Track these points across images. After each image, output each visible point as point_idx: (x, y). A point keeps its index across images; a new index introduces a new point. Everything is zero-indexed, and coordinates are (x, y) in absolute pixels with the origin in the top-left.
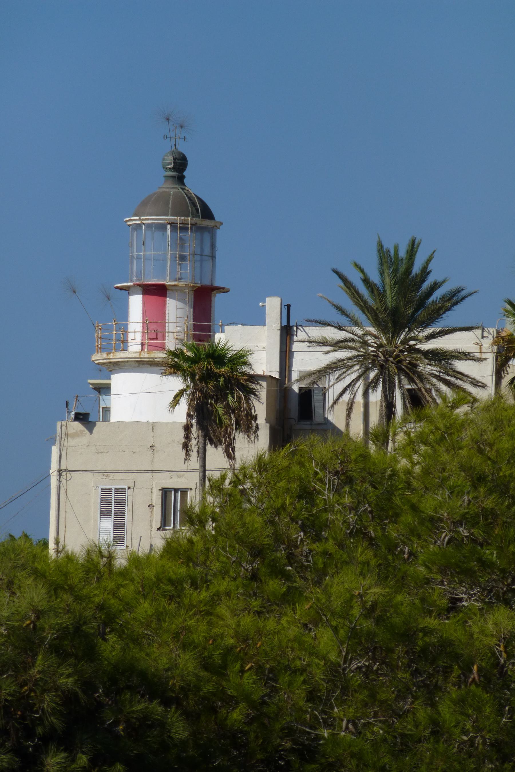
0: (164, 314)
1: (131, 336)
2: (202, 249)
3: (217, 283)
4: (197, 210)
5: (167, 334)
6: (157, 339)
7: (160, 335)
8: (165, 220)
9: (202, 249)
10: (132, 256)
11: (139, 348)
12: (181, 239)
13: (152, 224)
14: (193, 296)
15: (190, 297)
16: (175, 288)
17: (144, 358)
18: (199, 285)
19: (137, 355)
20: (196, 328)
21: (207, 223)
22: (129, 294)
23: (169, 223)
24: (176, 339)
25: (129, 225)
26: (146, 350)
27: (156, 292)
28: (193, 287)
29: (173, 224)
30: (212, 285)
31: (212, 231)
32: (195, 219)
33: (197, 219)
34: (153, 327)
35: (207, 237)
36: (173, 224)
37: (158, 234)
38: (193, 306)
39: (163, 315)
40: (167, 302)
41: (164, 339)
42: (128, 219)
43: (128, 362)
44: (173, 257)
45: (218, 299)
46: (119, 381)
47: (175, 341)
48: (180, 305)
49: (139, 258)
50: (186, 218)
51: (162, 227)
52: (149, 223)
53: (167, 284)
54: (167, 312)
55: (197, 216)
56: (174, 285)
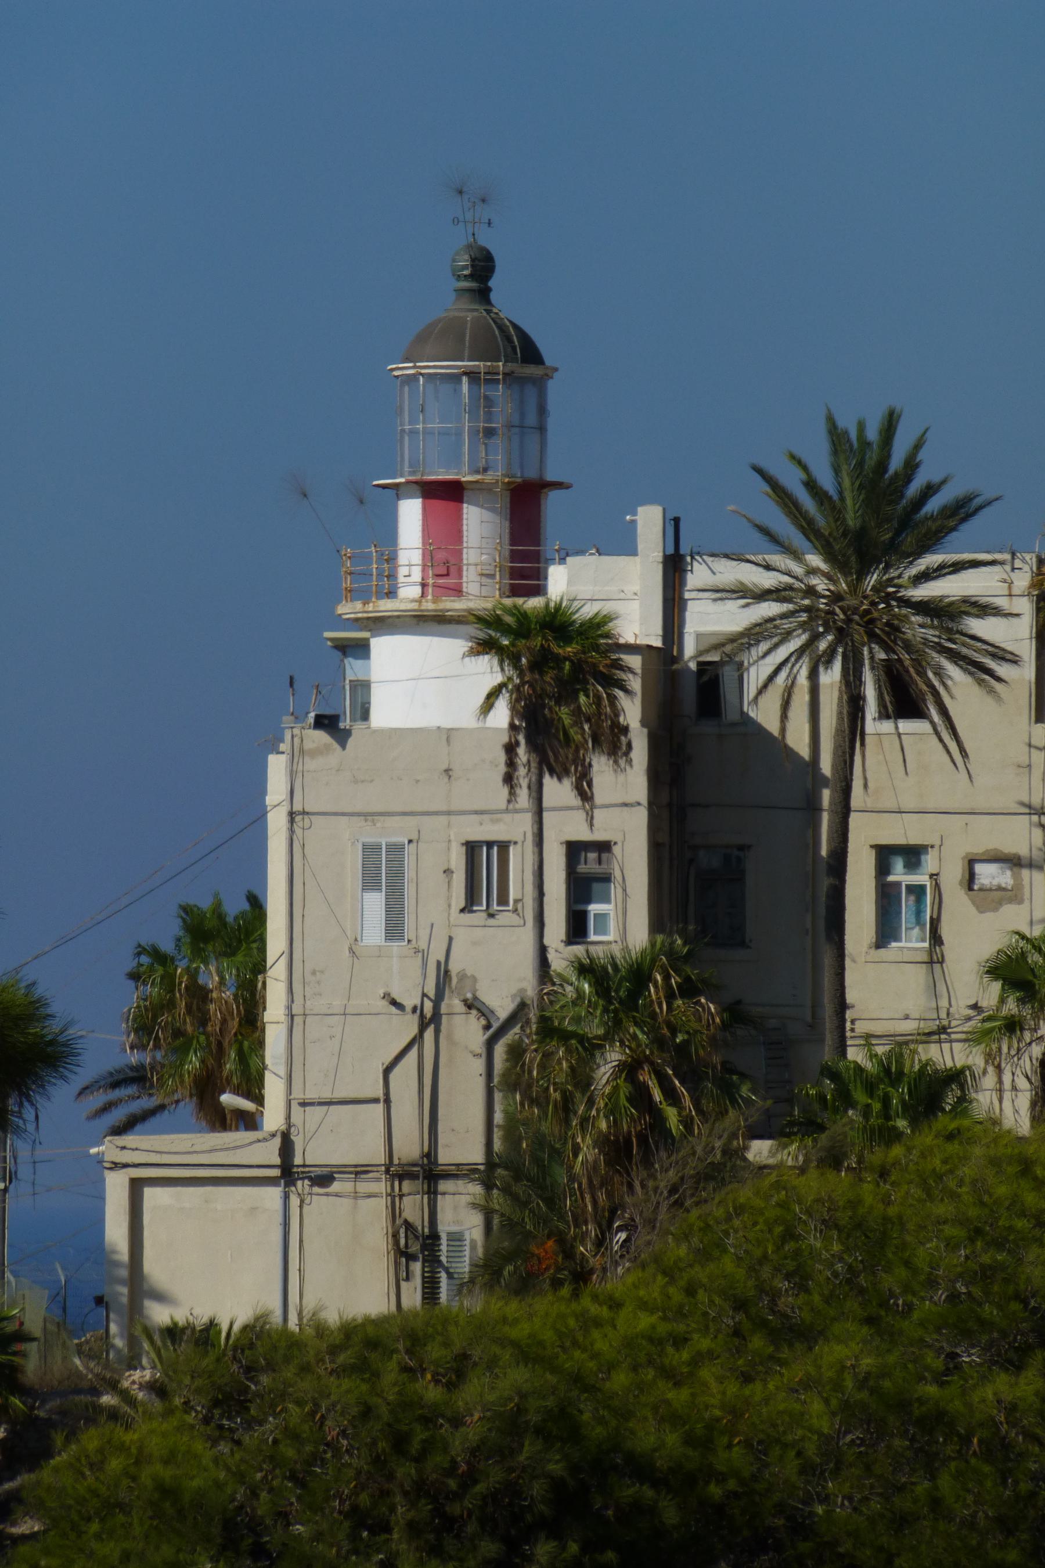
0: (460, 532)
1: (402, 571)
2: (522, 415)
3: (550, 477)
4: (514, 348)
5: (465, 568)
6: (448, 575)
7: (453, 570)
8: (459, 367)
9: (522, 415)
10: (403, 431)
11: (416, 591)
12: (486, 397)
13: (436, 374)
14: (508, 500)
15: (503, 502)
16: (478, 486)
17: (428, 611)
18: (519, 480)
19: (415, 606)
20: (514, 556)
21: (531, 370)
22: (398, 497)
23: (465, 373)
24: (482, 575)
25: (397, 377)
26: (430, 597)
27: (443, 494)
28: (509, 483)
29: (472, 375)
30: (541, 478)
31: (540, 384)
32: (510, 364)
33: (515, 364)
34: (441, 555)
35: (531, 392)
36: (472, 375)
37: (446, 388)
38: (508, 516)
39: (457, 536)
40: (465, 511)
41: (460, 577)
42: (394, 366)
43: (398, 617)
44: (474, 432)
45: (553, 503)
46: (382, 646)
47: (478, 578)
48: (487, 515)
49: (413, 432)
50: (495, 364)
51: (454, 379)
52: (430, 374)
53: (463, 479)
54: (465, 528)
55: (514, 360)
56: (476, 482)
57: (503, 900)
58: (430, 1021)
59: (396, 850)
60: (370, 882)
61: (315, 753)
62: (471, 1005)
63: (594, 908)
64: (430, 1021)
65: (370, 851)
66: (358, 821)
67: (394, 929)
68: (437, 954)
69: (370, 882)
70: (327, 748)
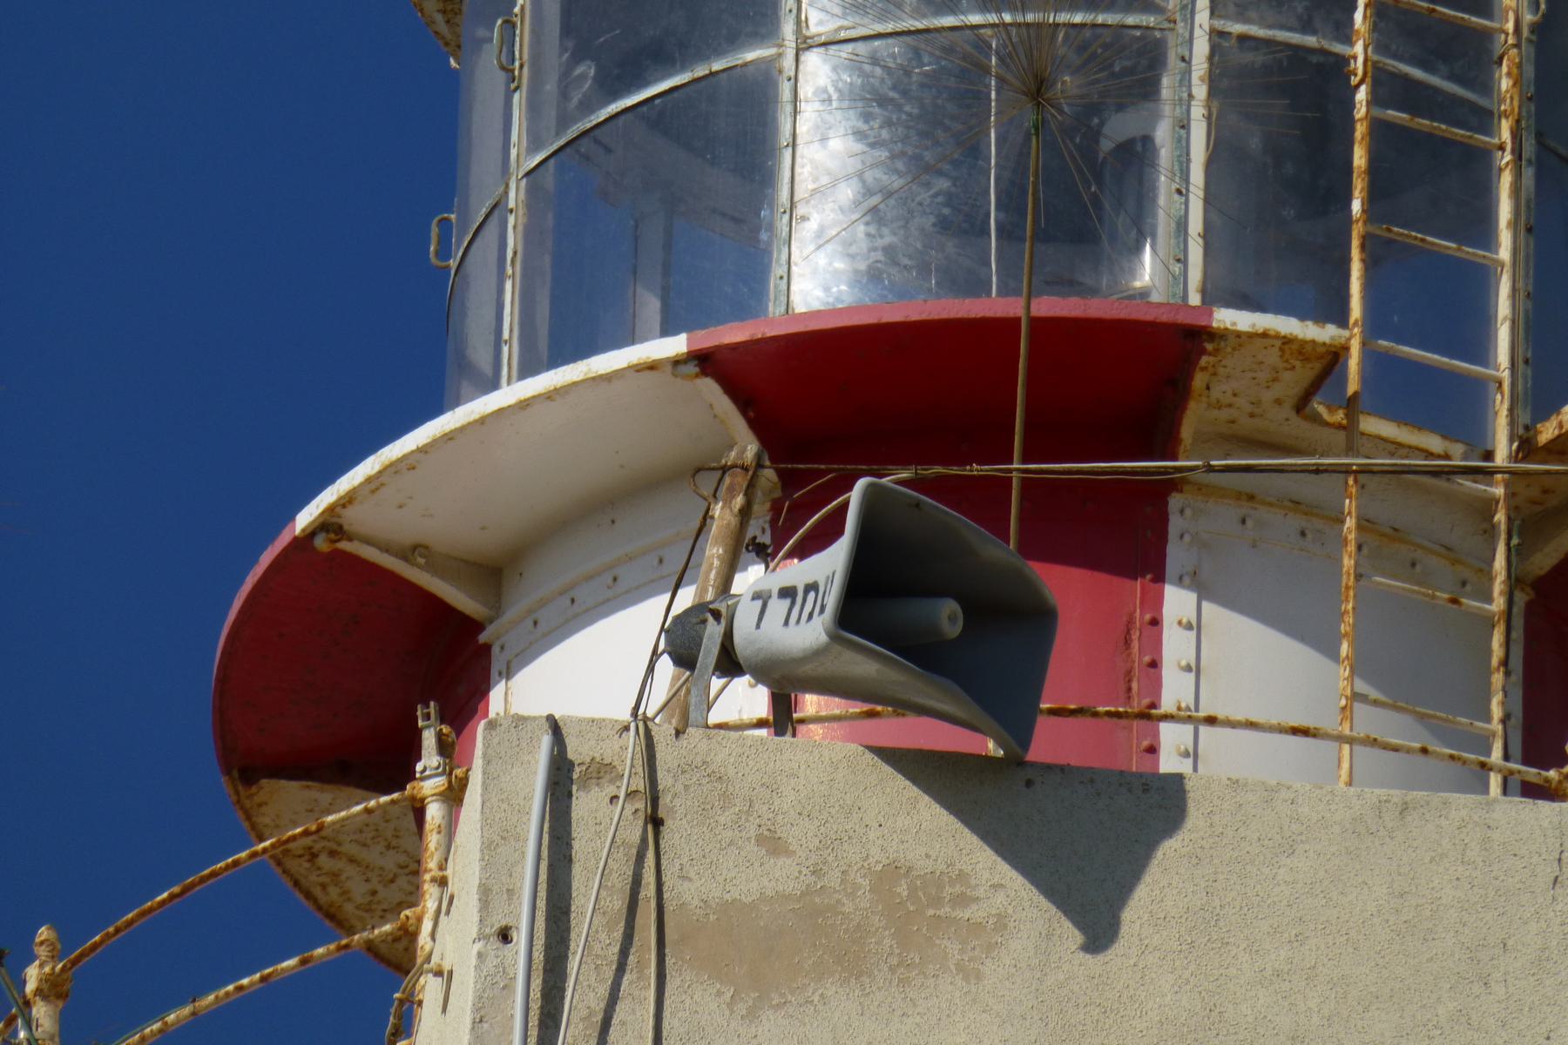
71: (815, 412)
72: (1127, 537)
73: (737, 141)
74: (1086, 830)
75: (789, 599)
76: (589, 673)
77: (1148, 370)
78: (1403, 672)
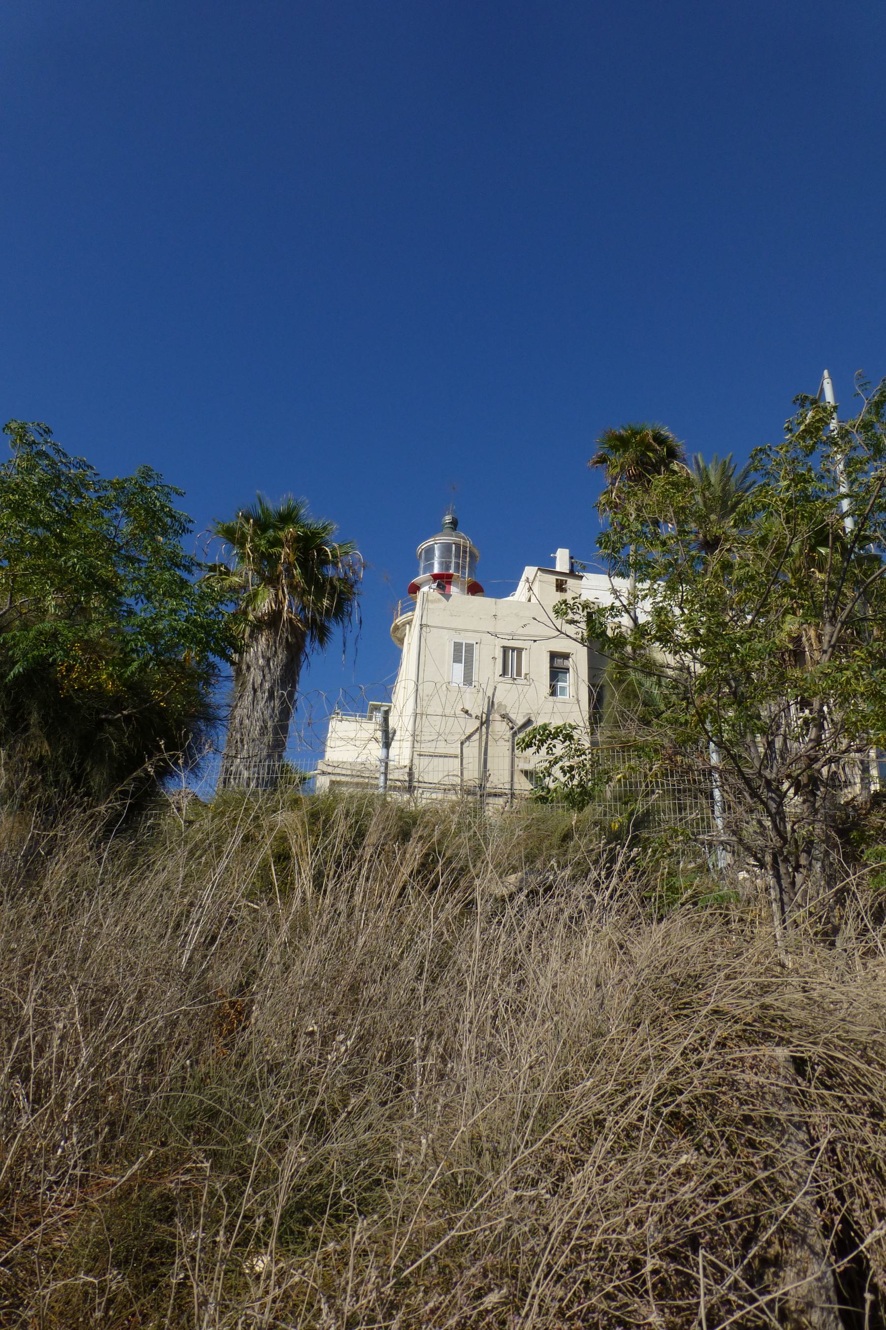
57: (519, 674)
58: (485, 722)
59: (470, 648)
60: (457, 660)
61: (433, 602)
62: (504, 716)
63: (560, 684)
64: (485, 722)
65: (457, 646)
66: (453, 632)
67: (468, 679)
68: (490, 693)
69: (457, 660)
70: (439, 600)
71: (436, 577)
72: (449, 583)
73: (432, 565)
74: (447, 597)
75: (434, 586)
76: (425, 589)
77: (450, 576)
78: (462, 590)
